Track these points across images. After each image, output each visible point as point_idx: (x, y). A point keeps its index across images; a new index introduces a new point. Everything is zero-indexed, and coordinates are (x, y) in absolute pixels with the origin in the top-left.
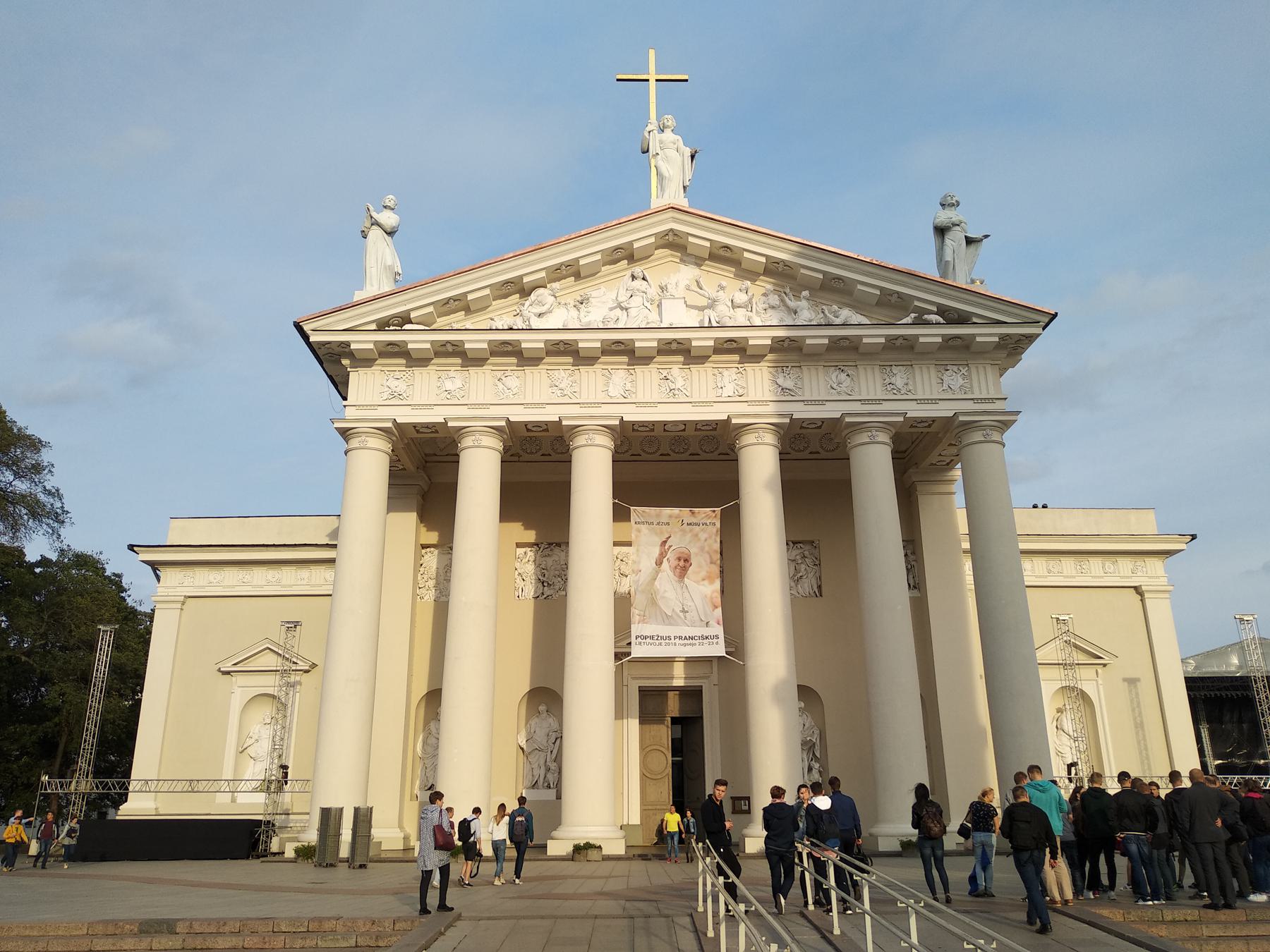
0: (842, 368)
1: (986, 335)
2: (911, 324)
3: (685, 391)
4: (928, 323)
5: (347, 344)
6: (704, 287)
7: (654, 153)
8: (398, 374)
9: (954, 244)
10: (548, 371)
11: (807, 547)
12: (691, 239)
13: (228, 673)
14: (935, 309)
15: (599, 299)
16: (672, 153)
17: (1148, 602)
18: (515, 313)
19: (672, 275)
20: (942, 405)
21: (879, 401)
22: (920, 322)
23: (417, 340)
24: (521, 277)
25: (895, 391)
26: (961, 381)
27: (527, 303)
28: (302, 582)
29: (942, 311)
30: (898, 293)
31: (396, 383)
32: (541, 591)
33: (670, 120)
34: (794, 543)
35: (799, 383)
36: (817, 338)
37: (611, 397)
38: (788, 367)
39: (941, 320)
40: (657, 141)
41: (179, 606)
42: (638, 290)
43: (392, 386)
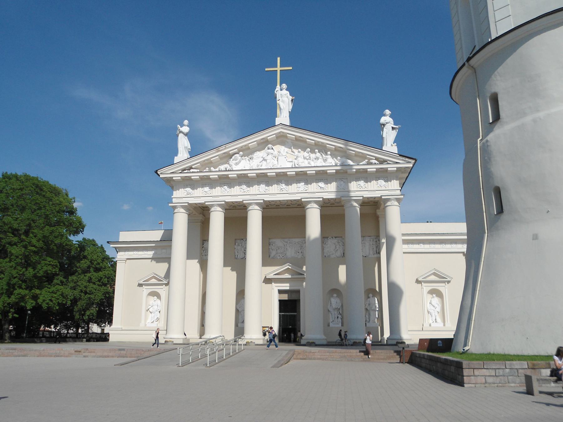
0: (342, 179)
2: (366, 164)
3: (286, 189)
4: (371, 164)
5: (172, 177)
8: (189, 186)
11: (340, 239)
14: (374, 158)
15: (256, 156)
16: (285, 99)
23: (195, 175)
25: (360, 187)
27: (232, 159)
29: (377, 159)
32: (243, 257)
33: (284, 86)
34: (335, 237)
39: (377, 162)
40: (280, 95)
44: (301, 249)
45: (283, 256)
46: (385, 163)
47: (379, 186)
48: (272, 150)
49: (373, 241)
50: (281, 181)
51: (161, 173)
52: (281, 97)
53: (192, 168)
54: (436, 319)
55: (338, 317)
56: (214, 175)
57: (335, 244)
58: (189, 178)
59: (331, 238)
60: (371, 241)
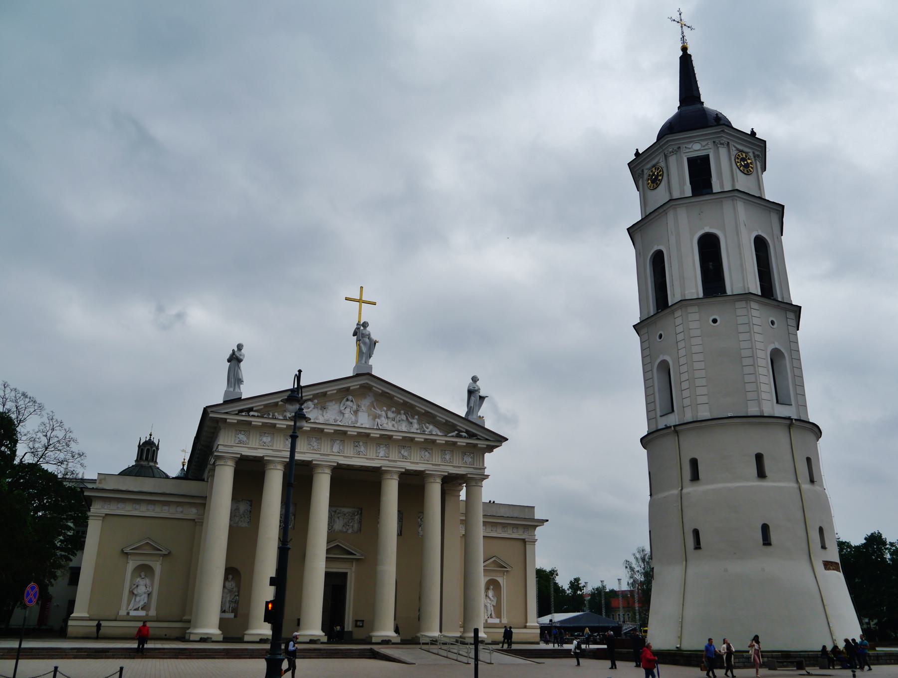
1: (482, 444)
4: (461, 437)
5: (226, 419)
6: (376, 407)
8: (243, 433)
12: (374, 388)
13: (127, 554)
17: (527, 545)
20: (463, 469)
21: (439, 465)
23: (257, 421)
26: (470, 460)
28: (165, 512)
29: (467, 432)
31: (242, 436)
36: (420, 438)
37: (333, 452)
41: (101, 518)
42: (349, 406)
43: (240, 438)
44: (352, 522)
45: (330, 528)
48: (352, 403)
52: (362, 337)
54: (491, 614)
58: (250, 423)
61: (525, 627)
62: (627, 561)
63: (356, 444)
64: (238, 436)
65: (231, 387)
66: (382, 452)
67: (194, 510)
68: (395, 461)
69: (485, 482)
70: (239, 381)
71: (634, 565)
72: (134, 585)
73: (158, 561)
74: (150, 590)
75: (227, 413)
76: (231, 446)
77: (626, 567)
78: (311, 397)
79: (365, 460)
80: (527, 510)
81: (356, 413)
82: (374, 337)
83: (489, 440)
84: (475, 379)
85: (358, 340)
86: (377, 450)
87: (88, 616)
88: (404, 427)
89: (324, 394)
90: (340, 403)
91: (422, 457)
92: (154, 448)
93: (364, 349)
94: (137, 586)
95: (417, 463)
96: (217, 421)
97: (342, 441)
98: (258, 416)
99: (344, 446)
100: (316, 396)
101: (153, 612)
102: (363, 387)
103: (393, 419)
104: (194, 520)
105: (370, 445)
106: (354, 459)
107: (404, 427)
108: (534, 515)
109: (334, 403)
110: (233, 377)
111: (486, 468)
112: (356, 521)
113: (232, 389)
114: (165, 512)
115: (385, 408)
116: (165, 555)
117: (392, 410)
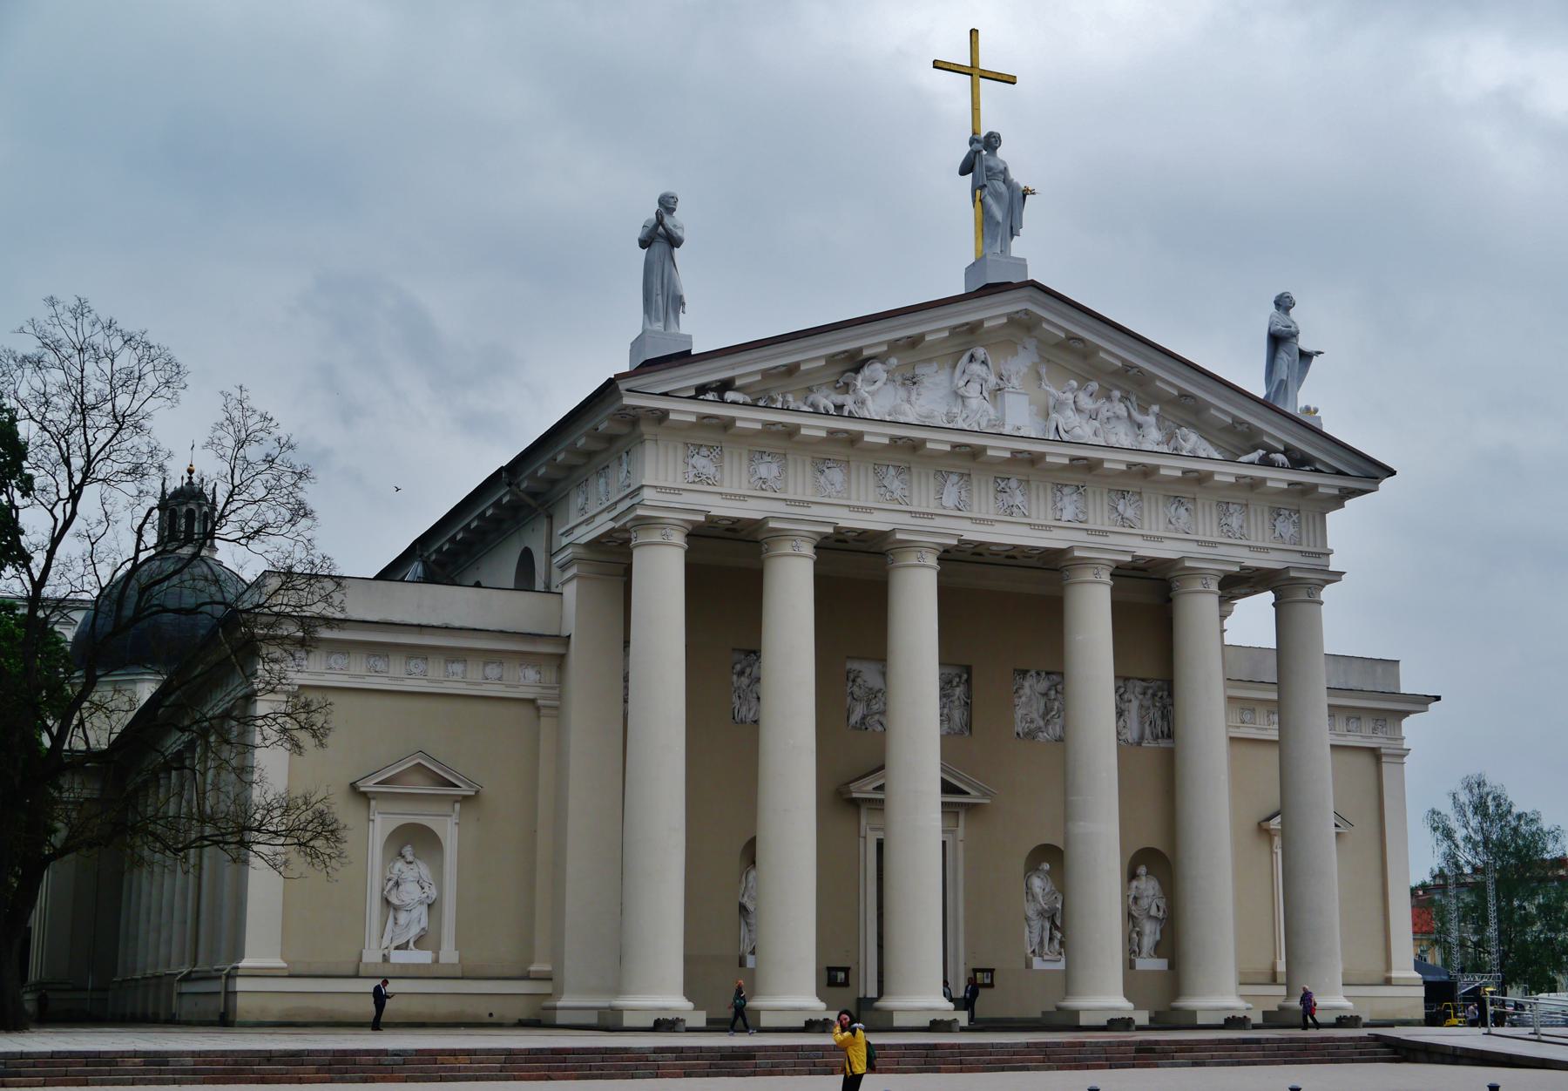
0: (1182, 500)
7: (981, 184)
8: (704, 451)
9: (1289, 358)
10: (876, 467)
12: (1045, 326)
13: (364, 794)
14: (1282, 449)
17: (1385, 767)
18: (838, 385)
19: (1009, 358)
21: (1214, 544)
22: (1266, 462)
23: (750, 419)
24: (860, 350)
25: (1230, 534)
26: (1292, 530)
27: (860, 377)
28: (455, 678)
29: (1288, 451)
30: (1249, 423)
31: (704, 461)
34: (1048, 673)
35: (1138, 512)
36: (1171, 468)
37: (944, 508)
38: (1128, 492)
39: (1287, 463)
42: (979, 376)
43: (698, 466)
46: (1308, 468)
47: (1277, 534)
48: (985, 368)
49: (1154, 695)
50: (1009, 479)
51: (628, 390)
53: (730, 389)
55: (1051, 939)
56: (814, 427)
57: (1045, 694)
58: (727, 425)
59: (1034, 675)
60: (1149, 696)
61: (1388, 982)
62: (1434, 812)
63: (1003, 485)
64: (693, 461)
65: (659, 320)
66: (1069, 506)
67: (531, 674)
68: (1104, 533)
69: (1327, 593)
70: (676, 303)
71: (1454, 823)
72: (389, 880)
73: (450, 816)
74: (433, 893)
75: (665, 394)
76: (678, 491)
77: (1435, 829)
78: (885, 348)
79: (1025, 530)
80: (1379, 669)
81: (995, 396)
82: (1019, 177)
83: (1349, 475)
84: (1283, 303)
85: (977, 187)
86: (1055, 503)
87: (285, 965)
88: (1122, 436)
89: (914, 342)
90: (954, 367)
91: (1171, 523)
92: (205, 509)
93: (998, 213)
94: (397, 884)
95: (1160, 539)
96: (634, 418)
97: (965, 476)
98: (744, 404)
99: (969, 491)
100: (895, 347)
101: (449, 955)
102: (1013, 321)
103: (1093, 416)
104: (533, 701)
105: (1038, 487)
106: (998, 527)
107: (1122, 436)
108: (1398, 685)
109: (935, 366)
110: (659, 292)
111: (1331, 552)
112: (957, 703)
113: (659, 326)
114: (455, 678)
115: (1074, 384)
116: (466, 798)
117: (1090, 388)
